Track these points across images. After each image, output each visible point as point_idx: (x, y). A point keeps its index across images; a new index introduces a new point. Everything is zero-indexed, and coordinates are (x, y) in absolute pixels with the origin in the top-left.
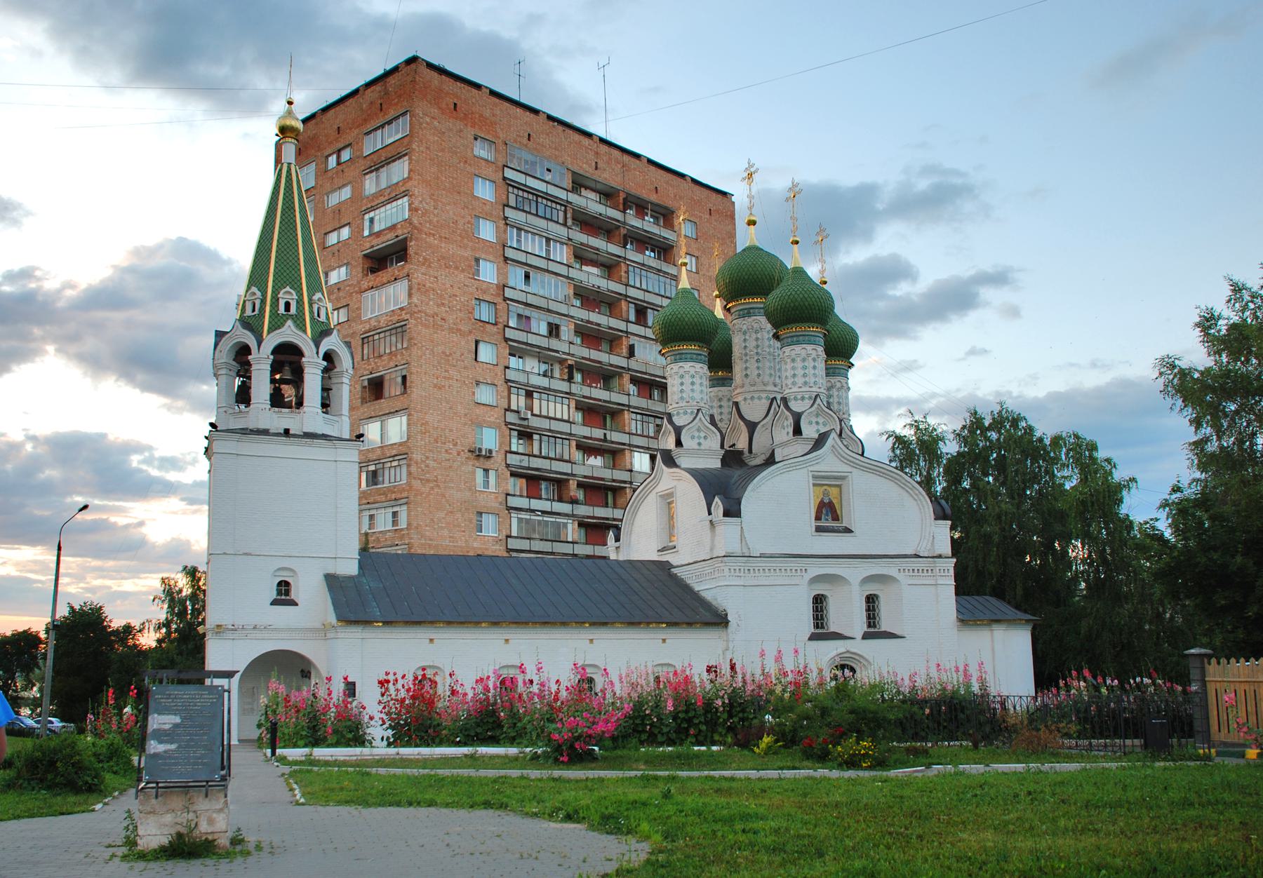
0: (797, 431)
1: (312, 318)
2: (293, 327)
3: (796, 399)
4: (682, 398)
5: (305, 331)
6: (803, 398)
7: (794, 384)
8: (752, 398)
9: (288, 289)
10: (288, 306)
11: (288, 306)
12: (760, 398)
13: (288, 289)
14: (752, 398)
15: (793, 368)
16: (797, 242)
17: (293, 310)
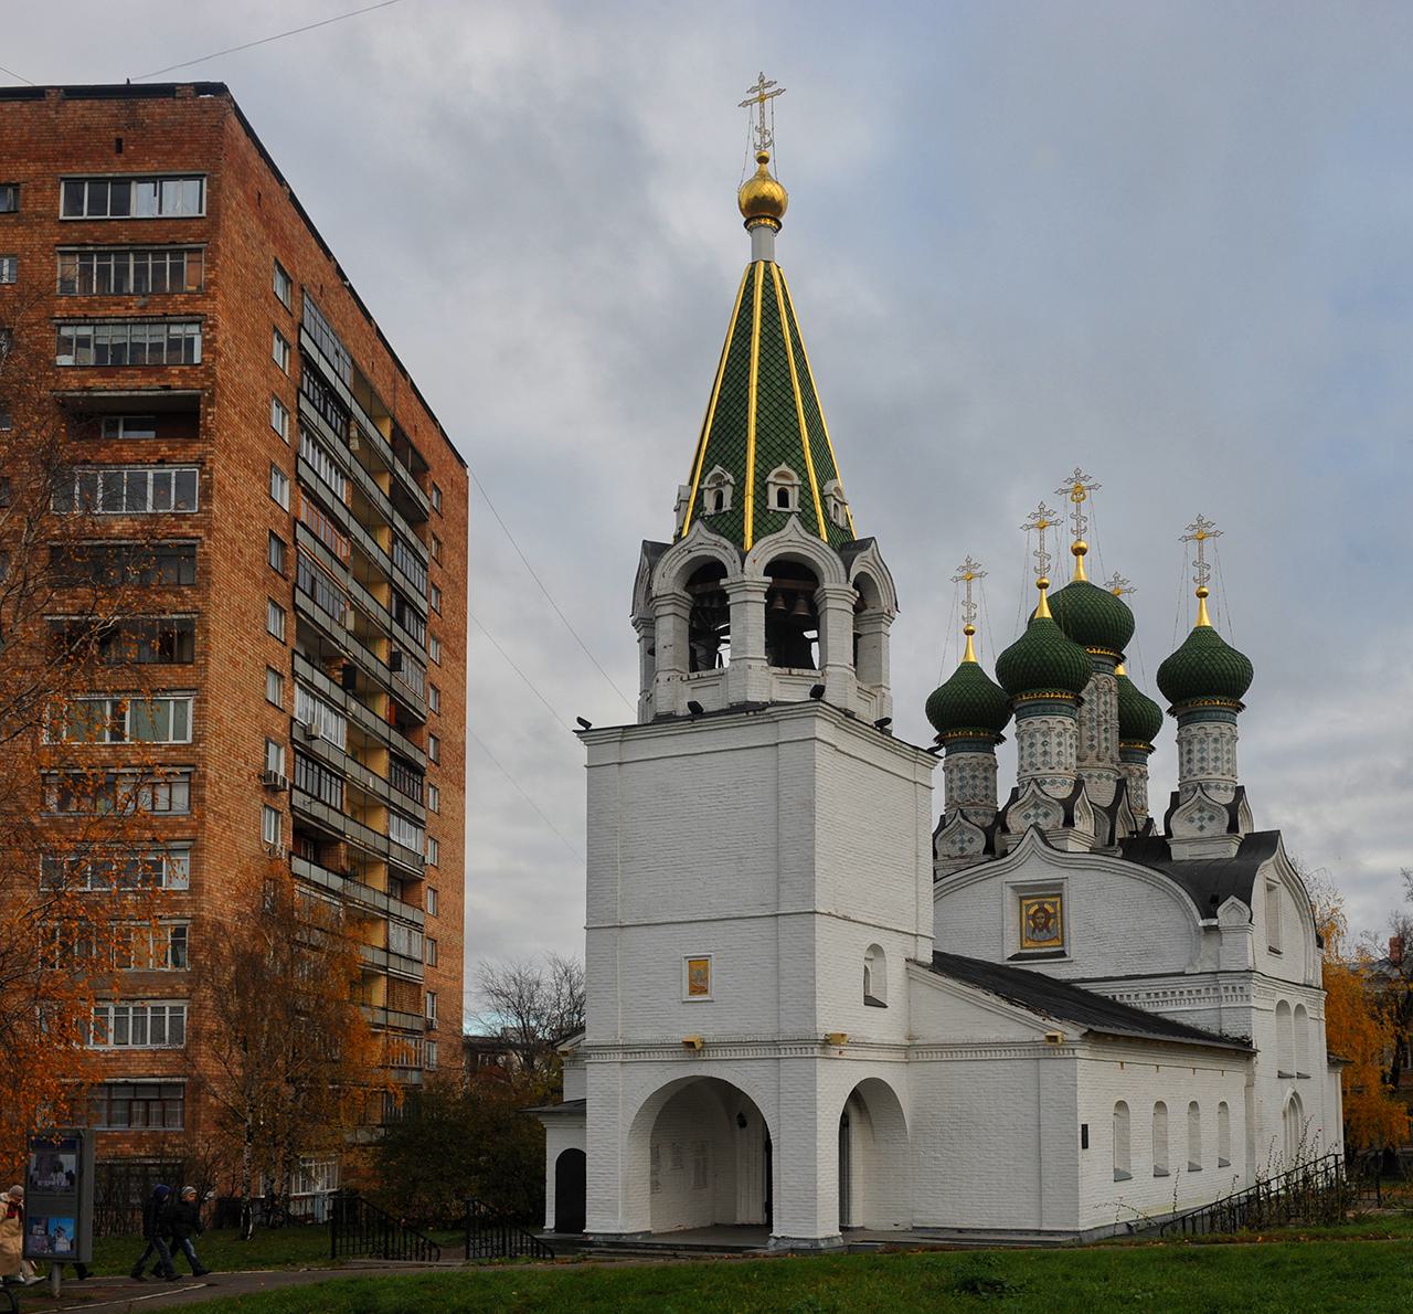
0: (1233, 827)
1: (829, 522)
2: (800, 527)
3: (1217, 788)
4: (1059, 763)
5: (818, 536)
6: (1226, 789)
7: (1216, 769)
8: (1100, 777)
9: (784, 467)
10: (783, 498)
11: (783, 498)
12: (1108, 778)
13: (784, 467)
14: (1100, 777)
15: (1215, 750)
16: (1204, 595)
17: (794, 504)
